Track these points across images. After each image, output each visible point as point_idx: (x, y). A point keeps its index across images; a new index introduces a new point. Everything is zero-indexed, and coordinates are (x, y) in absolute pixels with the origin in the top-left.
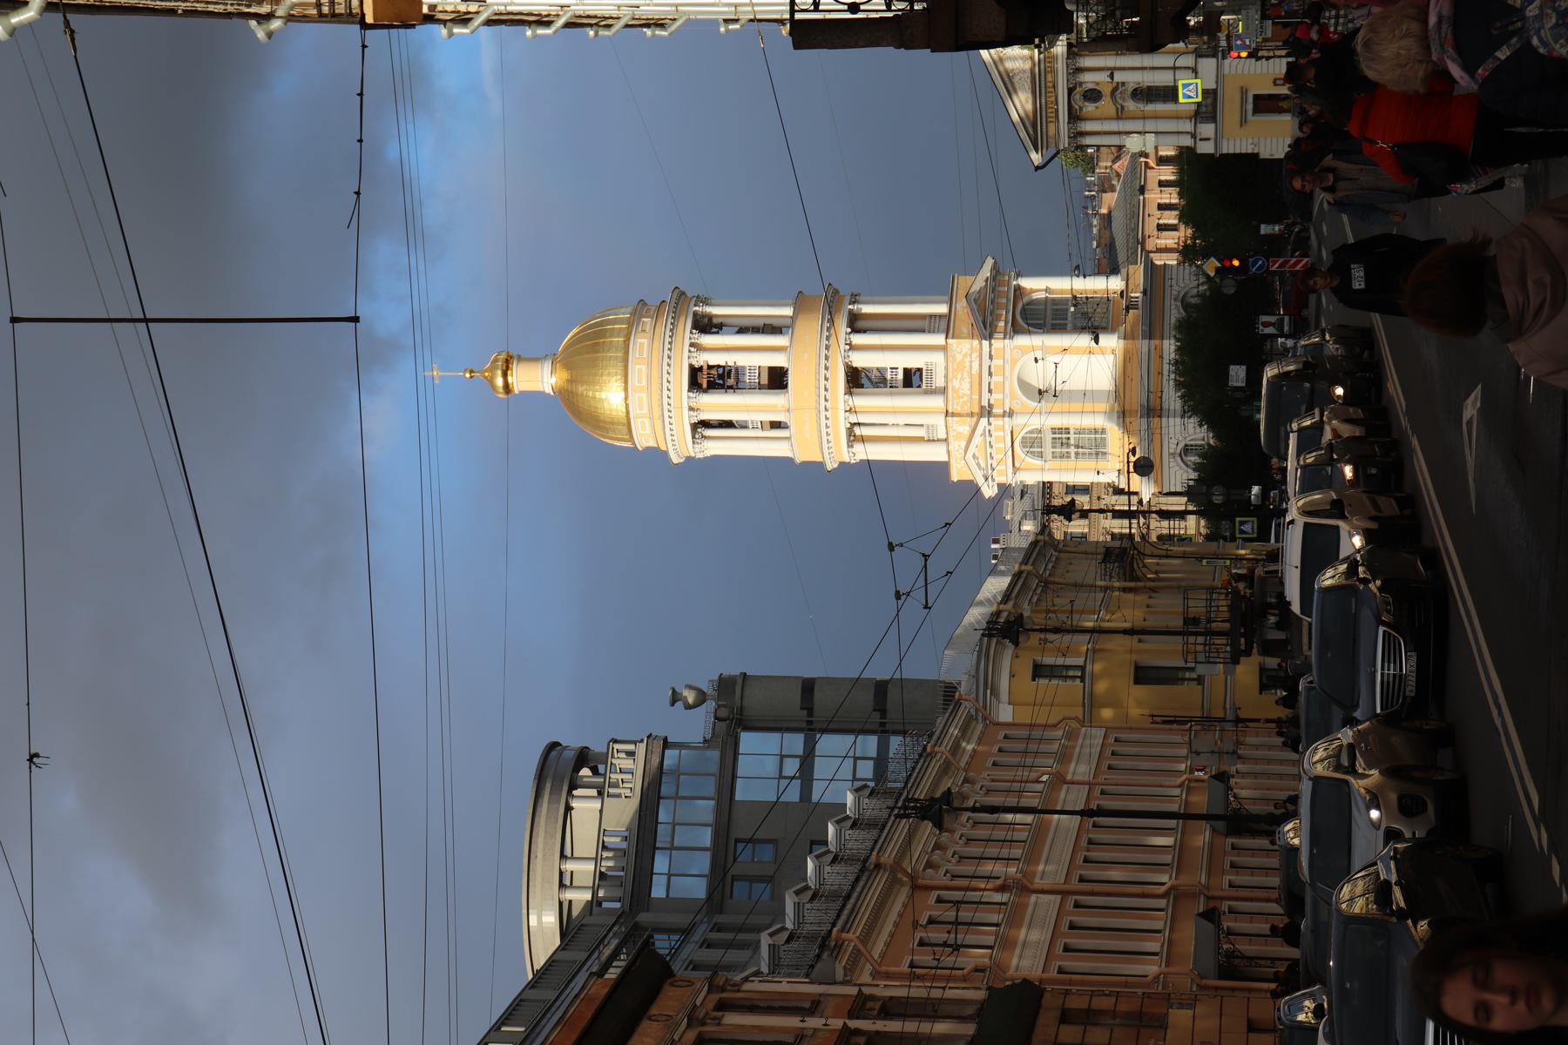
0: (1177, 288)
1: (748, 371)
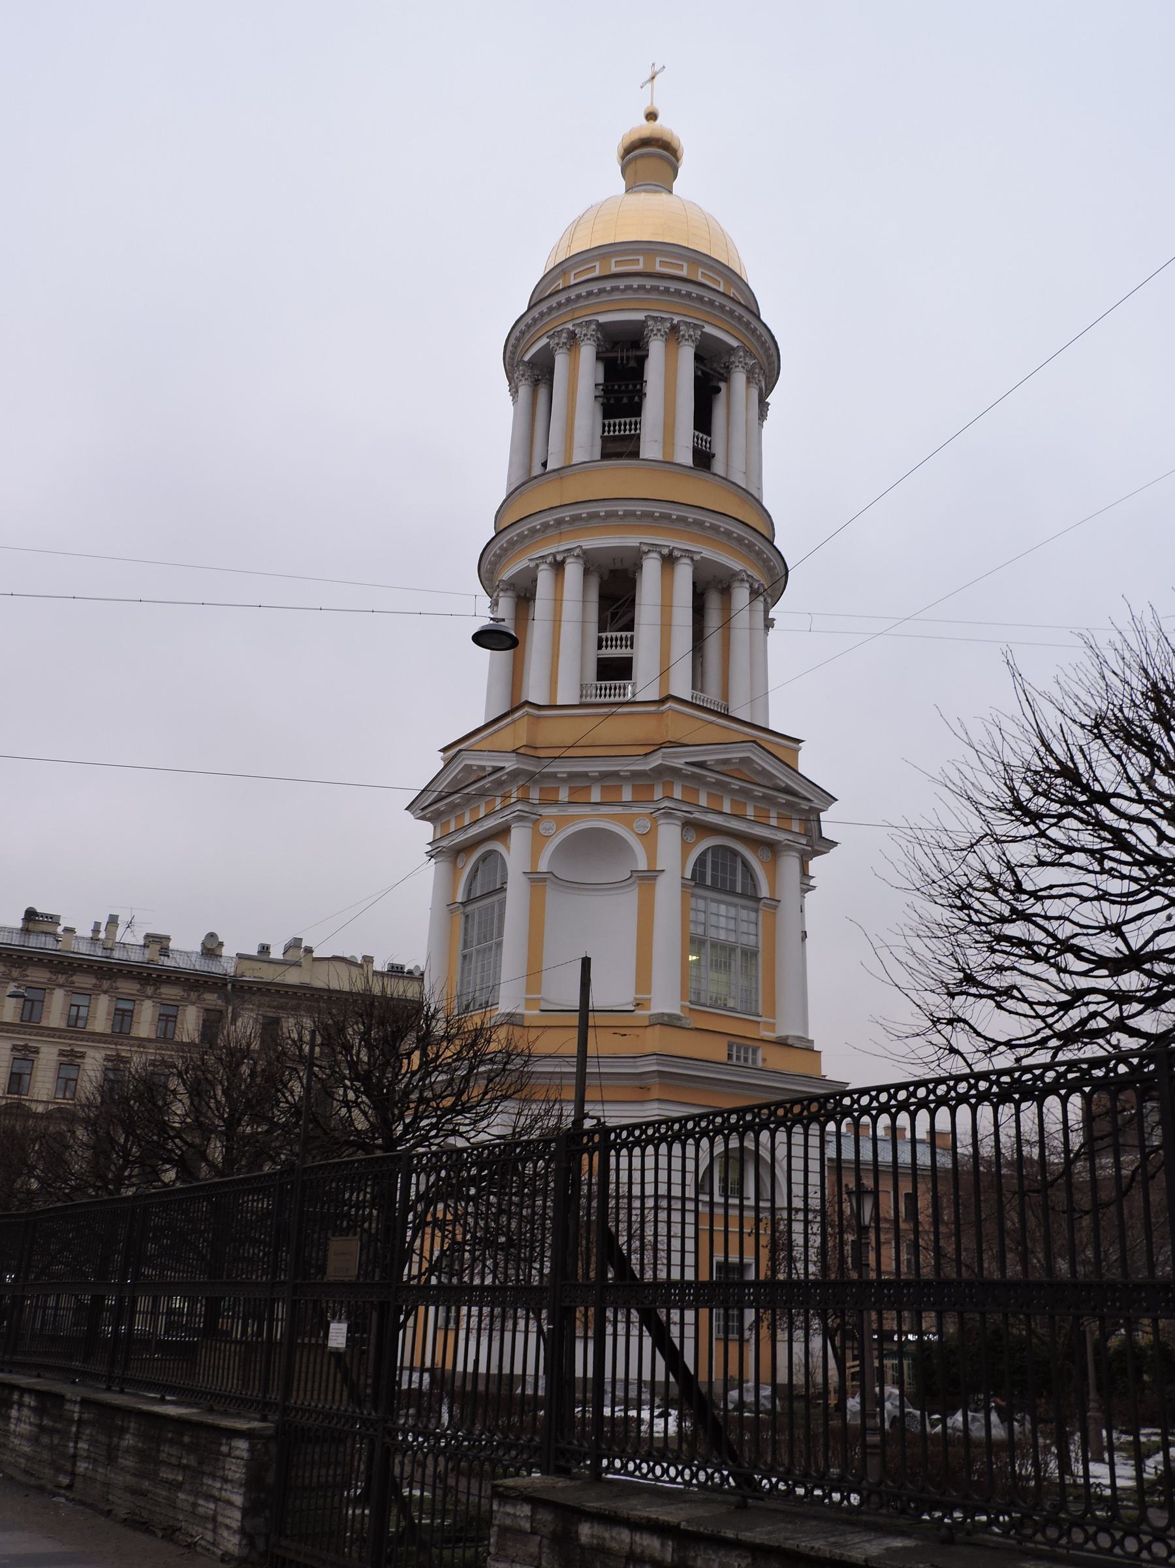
1: (633, 420)
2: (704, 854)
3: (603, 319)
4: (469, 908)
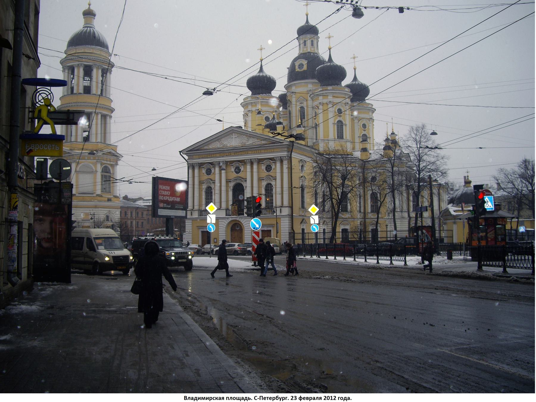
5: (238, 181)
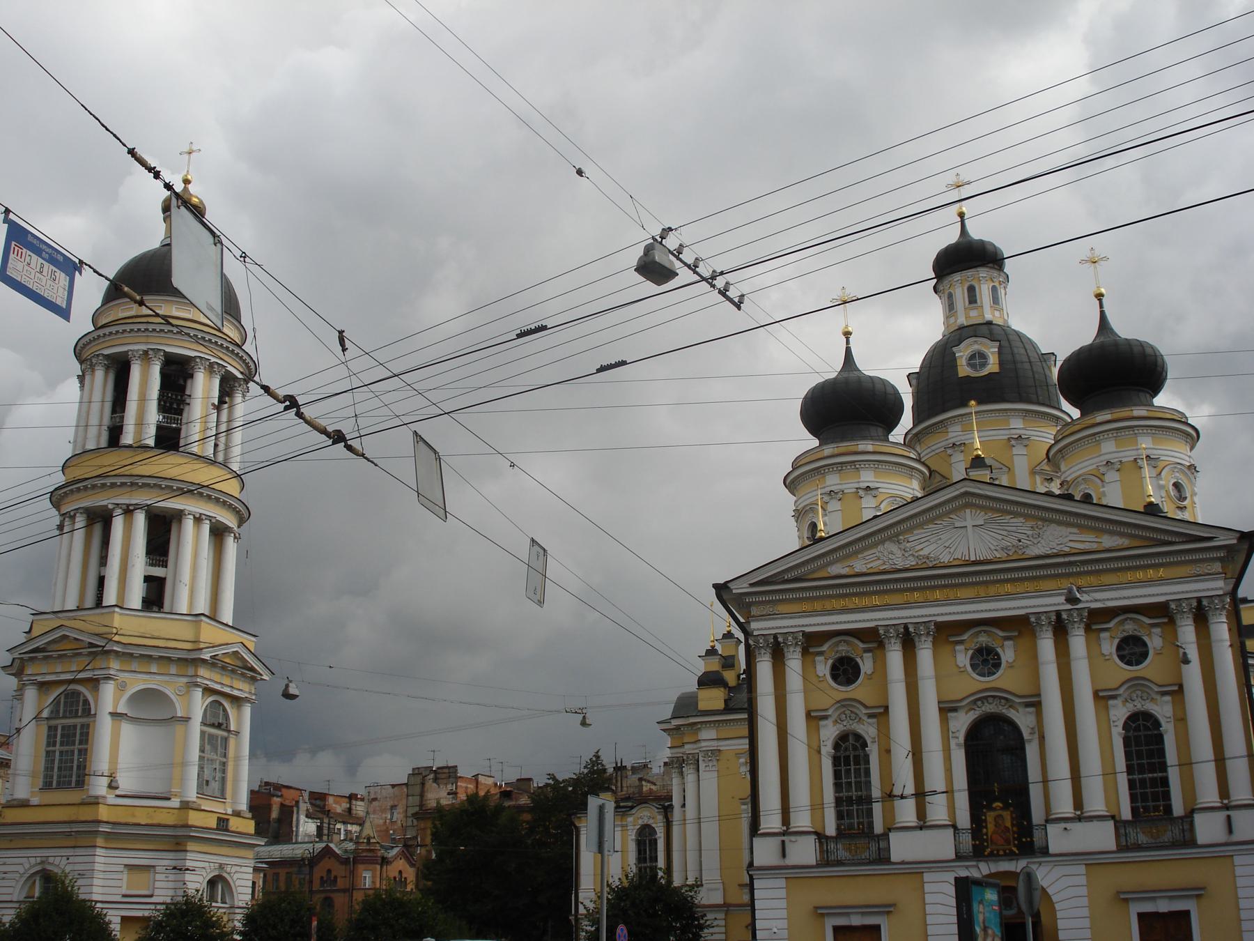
0: (233, 870)
2: (207, 706)
3: (168, 349)
4: (53, 722)
5: (990, 708)
